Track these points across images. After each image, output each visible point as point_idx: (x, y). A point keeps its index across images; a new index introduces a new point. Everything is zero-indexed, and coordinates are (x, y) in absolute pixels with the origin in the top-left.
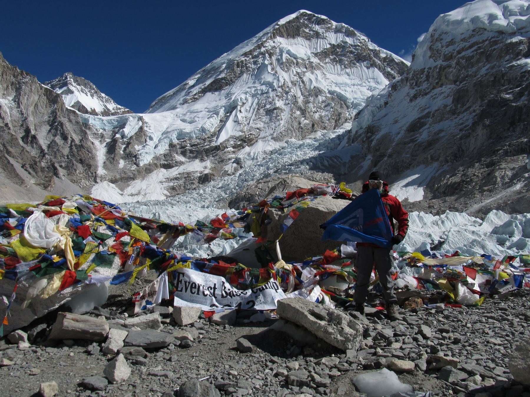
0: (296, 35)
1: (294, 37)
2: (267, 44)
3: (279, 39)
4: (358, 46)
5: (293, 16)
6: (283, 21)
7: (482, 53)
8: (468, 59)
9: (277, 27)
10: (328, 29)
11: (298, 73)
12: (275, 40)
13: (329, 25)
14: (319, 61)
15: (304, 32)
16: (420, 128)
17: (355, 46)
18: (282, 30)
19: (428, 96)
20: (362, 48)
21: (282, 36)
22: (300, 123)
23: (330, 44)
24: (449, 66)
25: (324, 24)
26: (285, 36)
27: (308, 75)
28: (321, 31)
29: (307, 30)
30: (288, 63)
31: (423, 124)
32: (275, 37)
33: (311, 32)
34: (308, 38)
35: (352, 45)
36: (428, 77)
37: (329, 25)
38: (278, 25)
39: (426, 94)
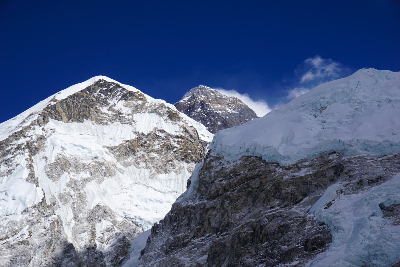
2: (29, 133)
3: (52, 123)
4: (182, 137)
6: (63, 95)
9: (53, 103)
10: (137, 109)
12: (46, 126)
13: (140, 102)
14: (115, 161)
15: (98, 111)
17: (177, 137)
18: (60, 110)
21: (58, 117)
25: (132, 99)
26: (65, 118)
28: (125, 111)
29: (104, 110)
32: (45, 120)
33: (110, 112)
35: (172, 136)
37: (140, 102)
38: (54, 100)
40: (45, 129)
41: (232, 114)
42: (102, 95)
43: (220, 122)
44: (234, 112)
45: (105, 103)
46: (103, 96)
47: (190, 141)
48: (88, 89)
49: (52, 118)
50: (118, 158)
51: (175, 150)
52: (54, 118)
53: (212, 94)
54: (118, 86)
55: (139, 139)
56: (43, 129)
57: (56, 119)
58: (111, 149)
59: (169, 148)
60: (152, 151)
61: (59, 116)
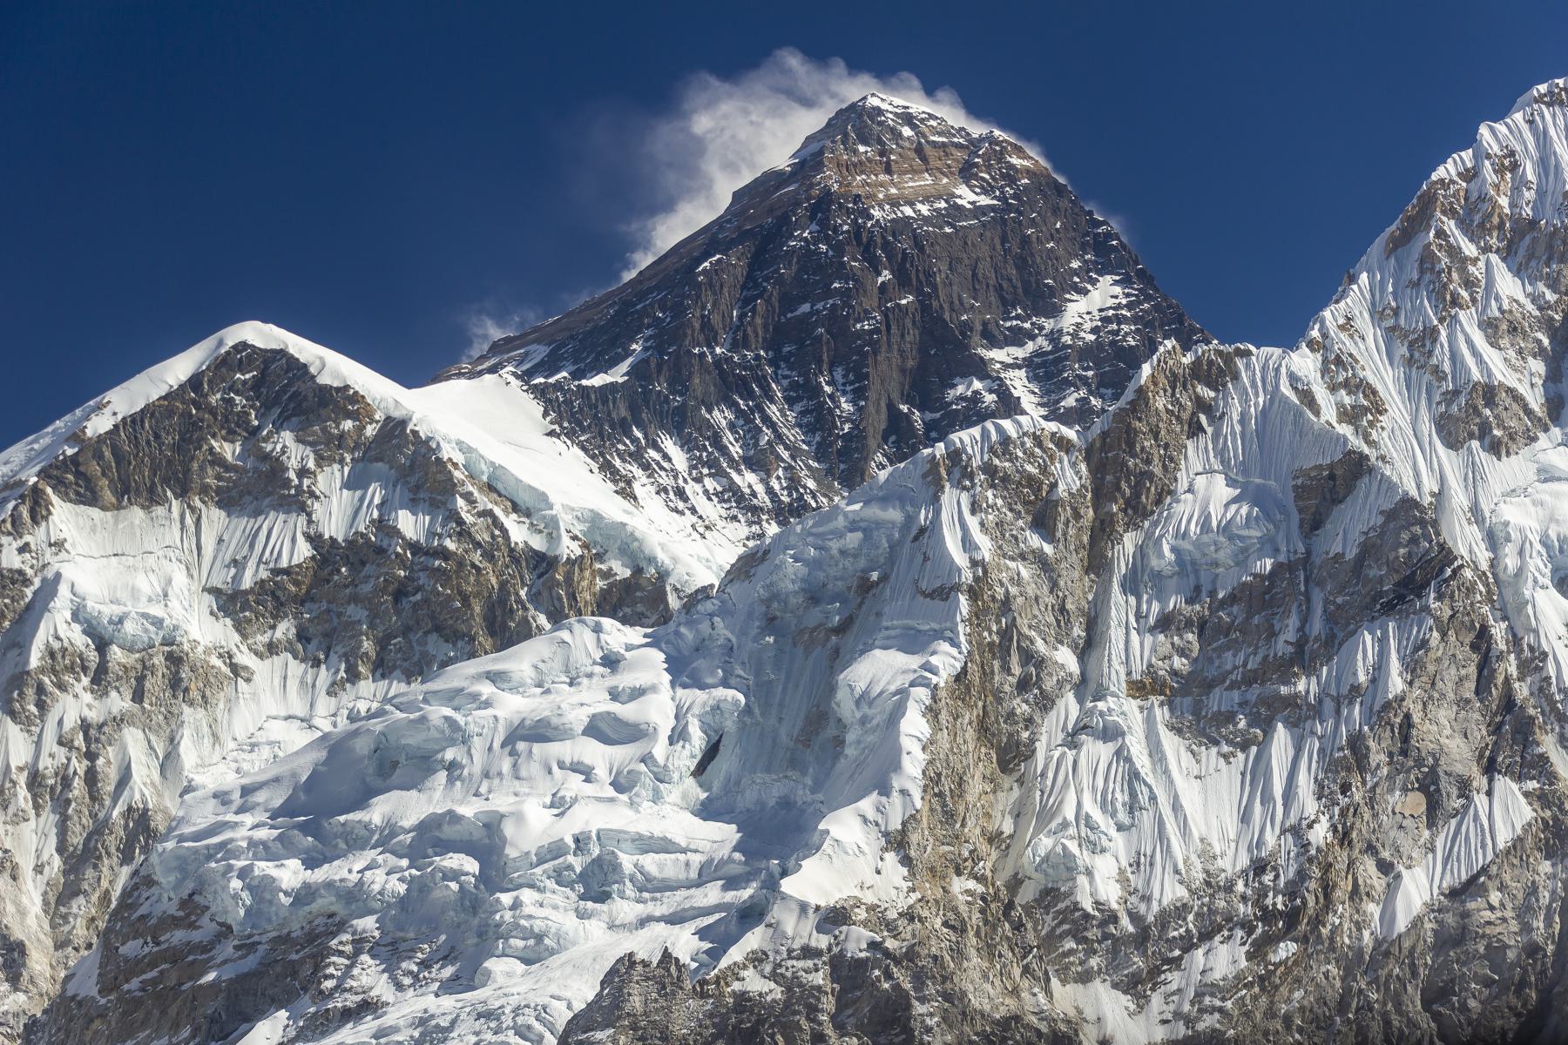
0: (166, 481)
1: (152, 499)
3: (64, 517)
4: (445, 554)
5: (178, 369)
11: (85, 726)
20: (461, 564)
21: (87, 496)
23: (315, 540)
26: (108, 496)
30: (54, 672)
38: (76, 437)
40: (33, 547)
41: (978, 211)
42: (238, 399)
43: (892, 272)
44: (984, 201)
47: (473, 566)
48: (195, 382)
49: (65, 497)
51: (419, 597)
52: (72, 496)
53: (907, 132)
57: (81, 500)
60: (355, 599)
61: (87, 489)
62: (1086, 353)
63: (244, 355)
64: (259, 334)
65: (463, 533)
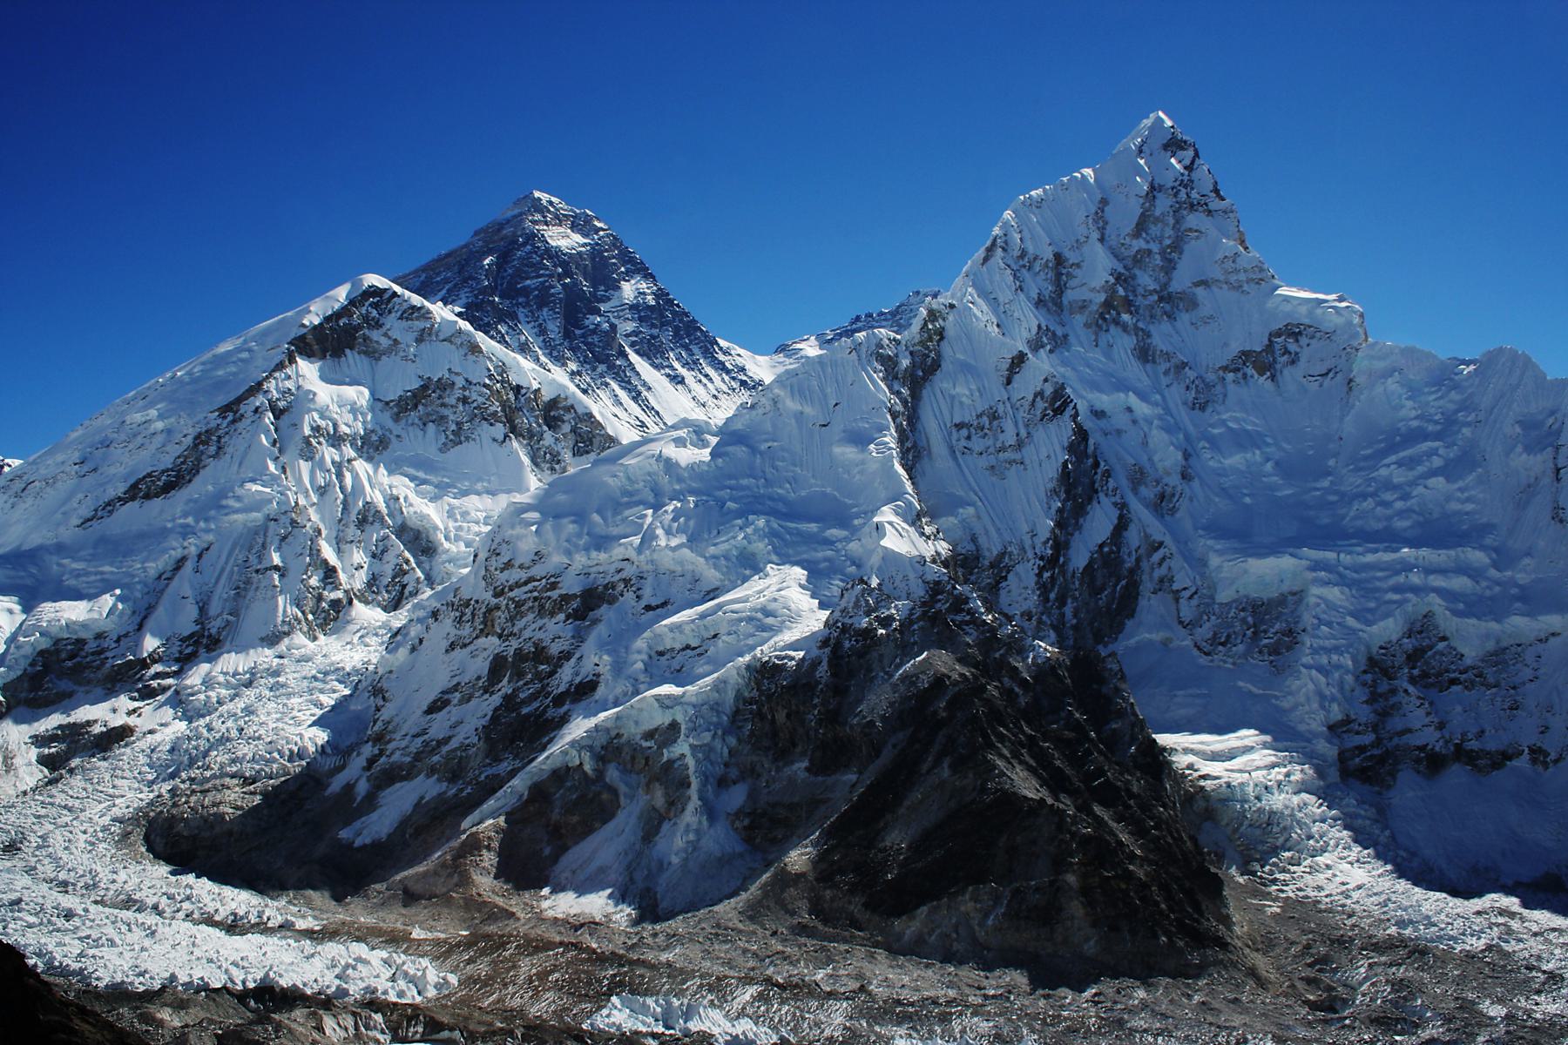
2: (271, 385)
4: (485, 386)
7: (535, 599)
8: (519, 604)
14: (390, 424)
16: (440, 709)
19: (470, 648)
21: (309, 354)
22: (320, 598)
24: (498, 608)
25: (417, 319)
27: (362, 466)
29: (375, 335)
31: (446, 703)
34: (373, 354)
36: (473, 615)
39: (465, 646)
41: (584, 245)
45: (378, 325)
46: (374, 313)
50: (396, 418)
54: (395, 294)
55: (424, 387)
56: (289, 377)
58: (387, 403)
59: (465, 400)
60: (443, 405)
62: (633, 307)
63: (375, 292)
64: (374, 280)
65: (490, 377)
